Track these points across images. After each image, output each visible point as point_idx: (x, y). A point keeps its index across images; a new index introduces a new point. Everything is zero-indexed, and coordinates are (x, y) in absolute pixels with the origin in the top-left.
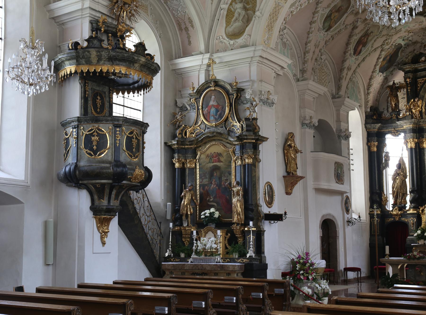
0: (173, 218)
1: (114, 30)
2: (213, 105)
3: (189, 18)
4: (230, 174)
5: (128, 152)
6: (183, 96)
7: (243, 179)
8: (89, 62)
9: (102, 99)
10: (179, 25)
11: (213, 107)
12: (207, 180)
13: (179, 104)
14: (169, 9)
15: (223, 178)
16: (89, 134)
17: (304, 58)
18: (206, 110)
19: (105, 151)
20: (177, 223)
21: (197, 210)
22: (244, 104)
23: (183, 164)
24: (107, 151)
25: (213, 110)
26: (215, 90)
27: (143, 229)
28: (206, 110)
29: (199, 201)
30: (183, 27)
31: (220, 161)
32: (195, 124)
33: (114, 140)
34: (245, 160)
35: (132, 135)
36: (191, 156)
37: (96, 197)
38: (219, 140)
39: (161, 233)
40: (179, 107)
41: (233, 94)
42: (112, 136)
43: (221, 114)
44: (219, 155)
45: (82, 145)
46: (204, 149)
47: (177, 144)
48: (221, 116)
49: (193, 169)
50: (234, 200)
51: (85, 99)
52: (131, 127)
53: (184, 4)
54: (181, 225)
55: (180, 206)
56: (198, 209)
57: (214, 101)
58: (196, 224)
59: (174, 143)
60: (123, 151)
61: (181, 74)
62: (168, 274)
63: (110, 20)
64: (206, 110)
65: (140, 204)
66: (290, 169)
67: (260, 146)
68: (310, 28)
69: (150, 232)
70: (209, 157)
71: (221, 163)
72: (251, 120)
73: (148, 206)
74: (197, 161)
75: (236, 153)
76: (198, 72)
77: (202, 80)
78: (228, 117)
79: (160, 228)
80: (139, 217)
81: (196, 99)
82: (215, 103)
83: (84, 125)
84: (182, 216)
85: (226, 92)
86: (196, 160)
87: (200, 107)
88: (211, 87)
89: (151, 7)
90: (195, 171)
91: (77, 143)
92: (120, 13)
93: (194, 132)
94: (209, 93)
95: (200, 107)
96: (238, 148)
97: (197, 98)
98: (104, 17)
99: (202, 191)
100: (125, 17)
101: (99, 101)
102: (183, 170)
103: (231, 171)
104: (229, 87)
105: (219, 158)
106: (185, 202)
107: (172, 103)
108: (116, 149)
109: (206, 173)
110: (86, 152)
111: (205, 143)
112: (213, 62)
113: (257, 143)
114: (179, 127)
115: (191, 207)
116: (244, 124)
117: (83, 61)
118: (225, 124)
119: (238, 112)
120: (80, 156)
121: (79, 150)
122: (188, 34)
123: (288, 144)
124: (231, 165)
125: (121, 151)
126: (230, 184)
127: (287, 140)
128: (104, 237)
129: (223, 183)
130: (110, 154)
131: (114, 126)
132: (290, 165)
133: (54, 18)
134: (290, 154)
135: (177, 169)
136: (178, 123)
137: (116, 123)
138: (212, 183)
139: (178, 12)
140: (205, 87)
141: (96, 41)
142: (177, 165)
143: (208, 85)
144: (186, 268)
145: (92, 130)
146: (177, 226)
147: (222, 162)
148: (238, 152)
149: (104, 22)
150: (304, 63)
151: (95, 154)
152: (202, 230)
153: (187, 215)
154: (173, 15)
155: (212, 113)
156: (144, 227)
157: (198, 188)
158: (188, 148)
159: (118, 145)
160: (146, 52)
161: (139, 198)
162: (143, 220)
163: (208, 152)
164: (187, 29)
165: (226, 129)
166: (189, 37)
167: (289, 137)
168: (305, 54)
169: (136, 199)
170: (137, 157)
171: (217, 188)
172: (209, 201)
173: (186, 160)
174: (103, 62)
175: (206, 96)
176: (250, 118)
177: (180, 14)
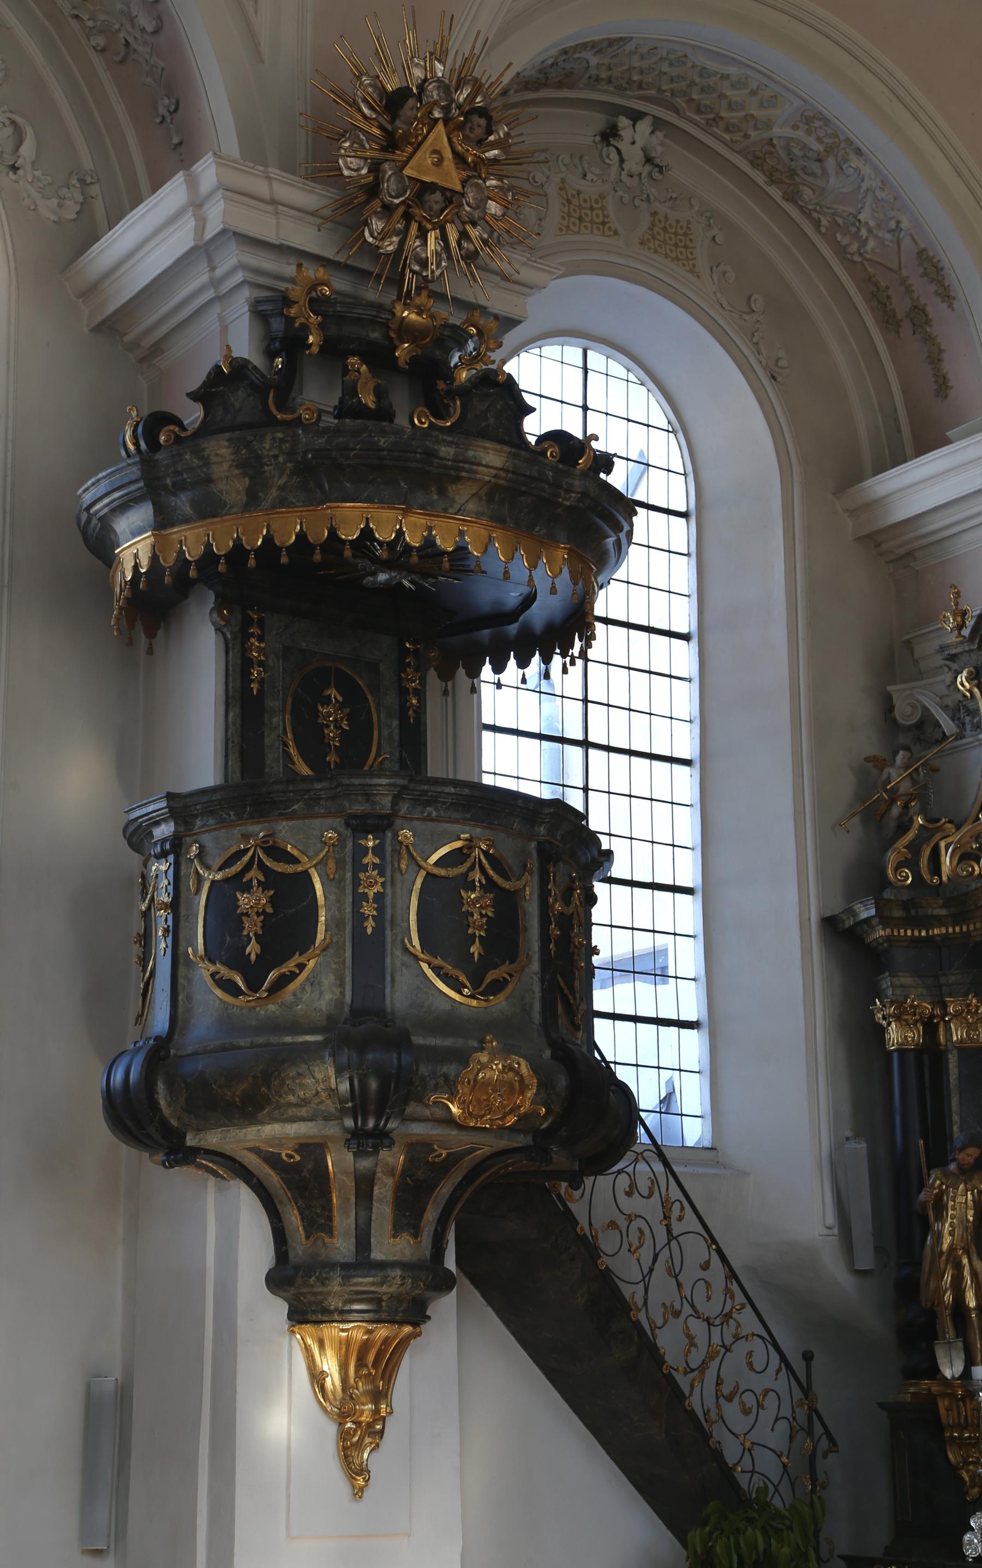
1: (375, 335)
3: (922, 254)
5: (438, 961)
8: (209, 509)
9: (354, 701)
10: (878, 299)
13: (904, 713)
14: (817, 224)
16: (226, 880)
19: (302, 967)
23: (930, 1027)
24: (311, 964)
27: (679, 1396)
30: (900, 306)
33: (349, 899)
35: (462, 869)
37: (293, 1219)
40: (909, 728)
42: (342, 879)
45: (193, 944)
51: (245, 709)
52: (457, 827)
53: (884, 183)
55: (919, 1264)
59: (864, 915)
60: (406, 959)
61: (909, 554)
63: (342, 283)
65: (646, 1255)
73: (706, 1266)
79: (807, 1391)
80: (637, 1325)
83: (206, 839)
84: (932, 1315)
89: (715, 231)
91: (175, 932)
92: (402, 243)
98: (312, 272)
100: (432, 260)
101: (331, 714)
106: (948, 1233)
108: (369, 952)
110: (213, 975)
114: (903, 827)
117: (183, 503)
120: (189, 998)
121: (182, 971)
122: (929, 339)
125: (394, 957)
128: (359, 1446)
130: (328, 980)
131: (348, 825)
133: (111, 327)
135: (895, 1055)
137: (359, 808)
139: (864, 233)
141: (241, 394)
142: (894, 1035)
145: (240, 854)
149: (317, 304)
151: (254, 986)
154: (841, 252)
156: (683, 1382)
158: (945, 937)
159: (370, 926)
160: (533, 427)
161: (630, 1218)
162: (669, 1341)
164: (919, 317)
166: (935, 357)
169: (613, 1225)
170: (497, 987)
173: (944, 1006)
174: (274, 493)
177: (871, 244)
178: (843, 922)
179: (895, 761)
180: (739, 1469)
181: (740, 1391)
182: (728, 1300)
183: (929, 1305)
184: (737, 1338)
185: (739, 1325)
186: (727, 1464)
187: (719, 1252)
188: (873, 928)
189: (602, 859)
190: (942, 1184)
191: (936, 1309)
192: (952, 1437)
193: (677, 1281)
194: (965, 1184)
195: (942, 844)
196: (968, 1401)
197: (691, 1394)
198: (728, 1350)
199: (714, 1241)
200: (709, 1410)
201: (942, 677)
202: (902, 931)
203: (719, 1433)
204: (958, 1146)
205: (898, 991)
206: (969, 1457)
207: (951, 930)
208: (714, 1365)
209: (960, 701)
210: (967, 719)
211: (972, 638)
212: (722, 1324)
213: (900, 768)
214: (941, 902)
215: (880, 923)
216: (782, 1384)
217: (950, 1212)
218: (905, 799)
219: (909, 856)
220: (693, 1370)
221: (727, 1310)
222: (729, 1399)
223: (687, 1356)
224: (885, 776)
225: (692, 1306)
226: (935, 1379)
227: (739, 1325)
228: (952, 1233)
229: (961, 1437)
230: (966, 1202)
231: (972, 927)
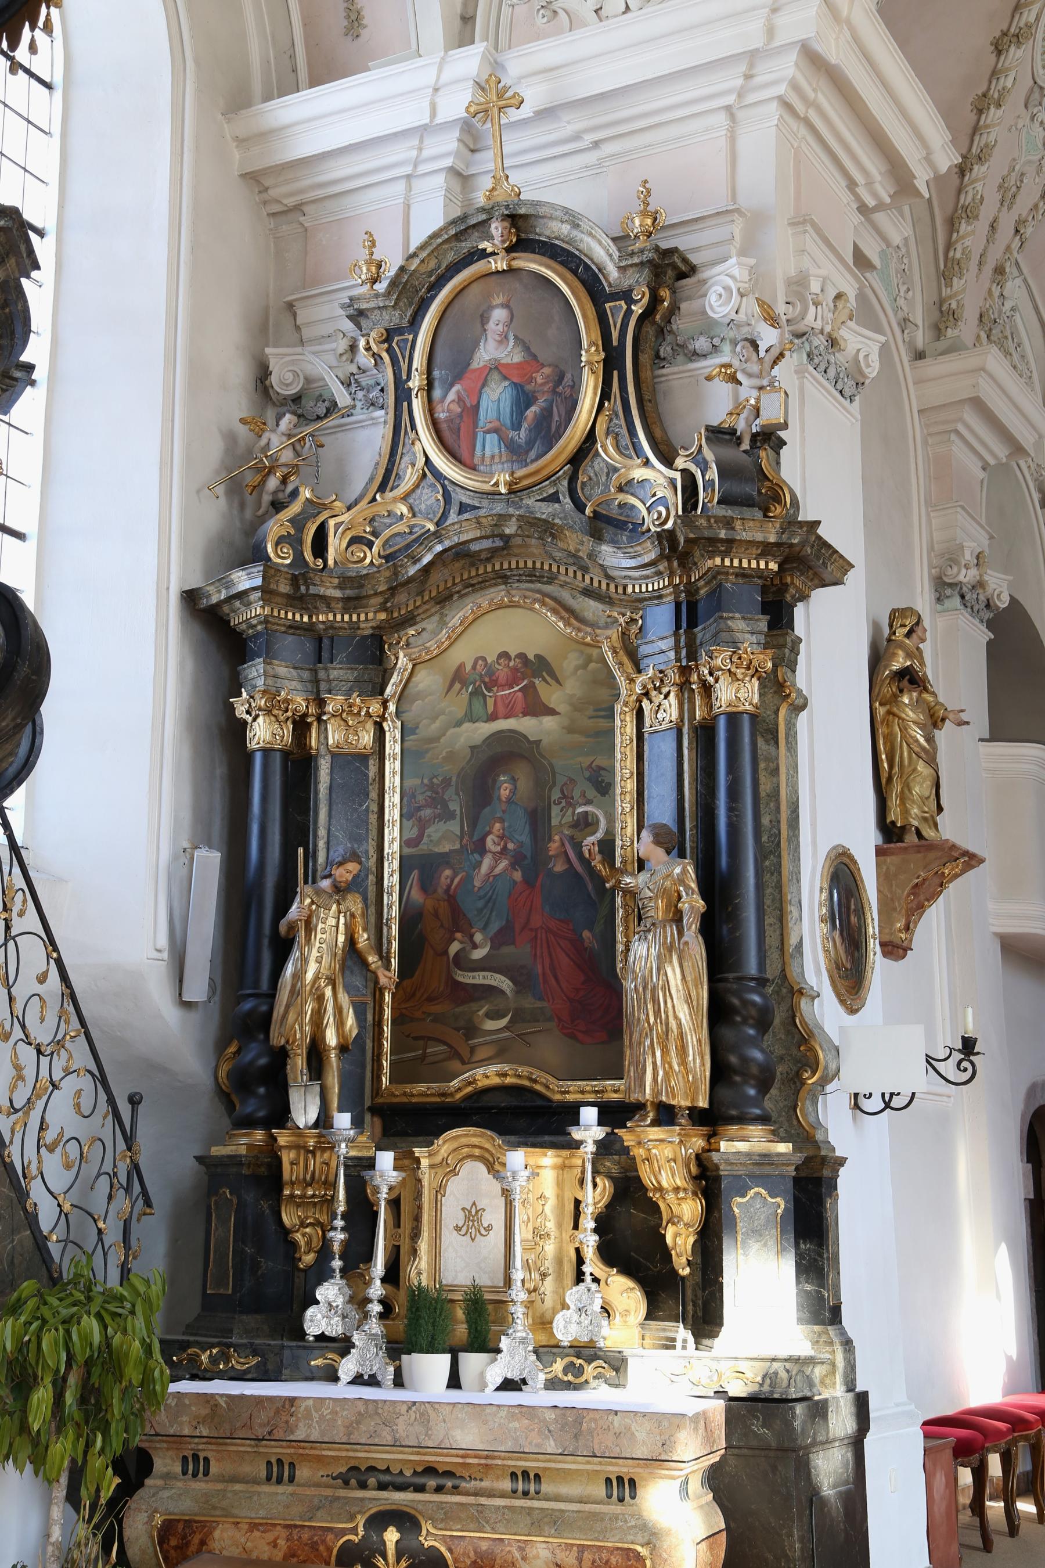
0: (222, 1073)
2: (497, 368)
4: (603, 786)
6: (306, 333)
7: (695, 816)
11: (496, 376)
12: (454, 827)
13: (284, 380)
15: (555, 810)
17: (949, 246)
18: (452, 396)
20: (250, 1107)
21: (378, 1024)
22: (696, 355)
25: (496, 398)
26: (511, 271)
28: (449, 401)
29: (394, 962)
31: (536, 708)
32: (382, 488)
34: (707, 689)
36: (351, 675)
38: (533, 576)
39: (135, 1168)
41: (627, 296)
43: (546, 415)
44: (535, 668)
46: (428, 635)
47: (267, 592)
48: (547, 432)
49: (363, 758)
50: (641, 954)
54: (279, 1115)
56: (388, 1013)
57: (504, 339)
58: (374, 1110)
61: (298, 208)
62: (167, 1476)
64: (452, 396)
66: (906, 812)
67: (799, 611)
68: (995, 74)
69: (52, 1163)
70: (464, 684)
71: (548, 722)
72: (746, 445)
73: (42, 979)
74: (392, 707)
75: (644, 650)
76: (400, 187)
77: (430, 216)
78: (591, 437)
79: (130, 1141)
81: (388, 336)
82: (511, 355)
84: (281, 1056)
85: (583, 282)
86: (385, 704)
87: (416, 382)
88: (483, 254)
90: (373, 771)
93: (375, 534)
94: (475, 288)
95: (416, 382)
96: (660, 619)
97: (399, 330)
99: (416, 895)
102: (297, 764)
103: (612, 771)
104: (601, 252)
105: (530, 691)
107: (239, 374)
109: (447, 782)
111: (444, 599)
112: (500, 96)
113: (784, 588)
115: (344, 999)
116: (705, 468)
118: (573, 479)
119: (653, 400)
123: (896, 666)
124: (612, 731)
126: (607, 847)
127: (876, 660)
129: (554, 847)
132: (907, 786)
134: (904, 729)
135: (258, 758)
136: (273, 483)
138: (481, 848)
140: (450, 257)
142: (262, 732)
143: (466, 246)
144: (300, 1434)
146: (247, 1123)
147: (552, 712)
148: (663, 645)
150: (948, 269)
152: (418, 1152)
153: (316, 1054)
155: (492, 415)
157: (392, 879)
158: (330, 626)
163: (463, 654)
165: (580, 507)
167: (901, 632)
168: (952, 224)
171: (518, 876)
172: (461, 961)
173: (321, 703)
175: (456, 305)
176: (741, 426)
178: (209, 596)
179: (278, 425)
180: (54, 1238)
181: (64, 1139)
182: (62, 1023)
183: (283, 1042)
184: (68, 1072)
185: (70, 1057)
186: (41, 1232)
187: (60, 963)
188: (248, 604)
189: (18, 374)
190: (313, 902)
191: (288, 1047)
192: (292, 1196)
193: (9, 993)
194: (339, 904)
195: (332, 523)
196: (318, 1154)
197: (11, 1142)
198: (55, 1086)
199: (56, 949)
200: (30, 1162)
201: (334, 345)
202: (283, 612)
203: (37, 1193)
205: (270, 682)
206: (307, 1218)
207: (339, 618)
208: (40, 1104)
209: (352, 374)
210: (360, 394)
211: (388, 293)
212: (52, 1053)
213: (283, 434)
214: (336, 581)
215: (262, 599)
216: (107, 1130)
217: (319, 936)
218: (286, 470)
219: (292, 532)
220: (16, 1111)
221: (59, 1037)
222: (51, 1149)
223: (12, 1092)
224: (263, 442)
225: (23, 1027)
227: (70, 1057)
229: (303, 1196)
230: (337, 926)
231: (363, 617)
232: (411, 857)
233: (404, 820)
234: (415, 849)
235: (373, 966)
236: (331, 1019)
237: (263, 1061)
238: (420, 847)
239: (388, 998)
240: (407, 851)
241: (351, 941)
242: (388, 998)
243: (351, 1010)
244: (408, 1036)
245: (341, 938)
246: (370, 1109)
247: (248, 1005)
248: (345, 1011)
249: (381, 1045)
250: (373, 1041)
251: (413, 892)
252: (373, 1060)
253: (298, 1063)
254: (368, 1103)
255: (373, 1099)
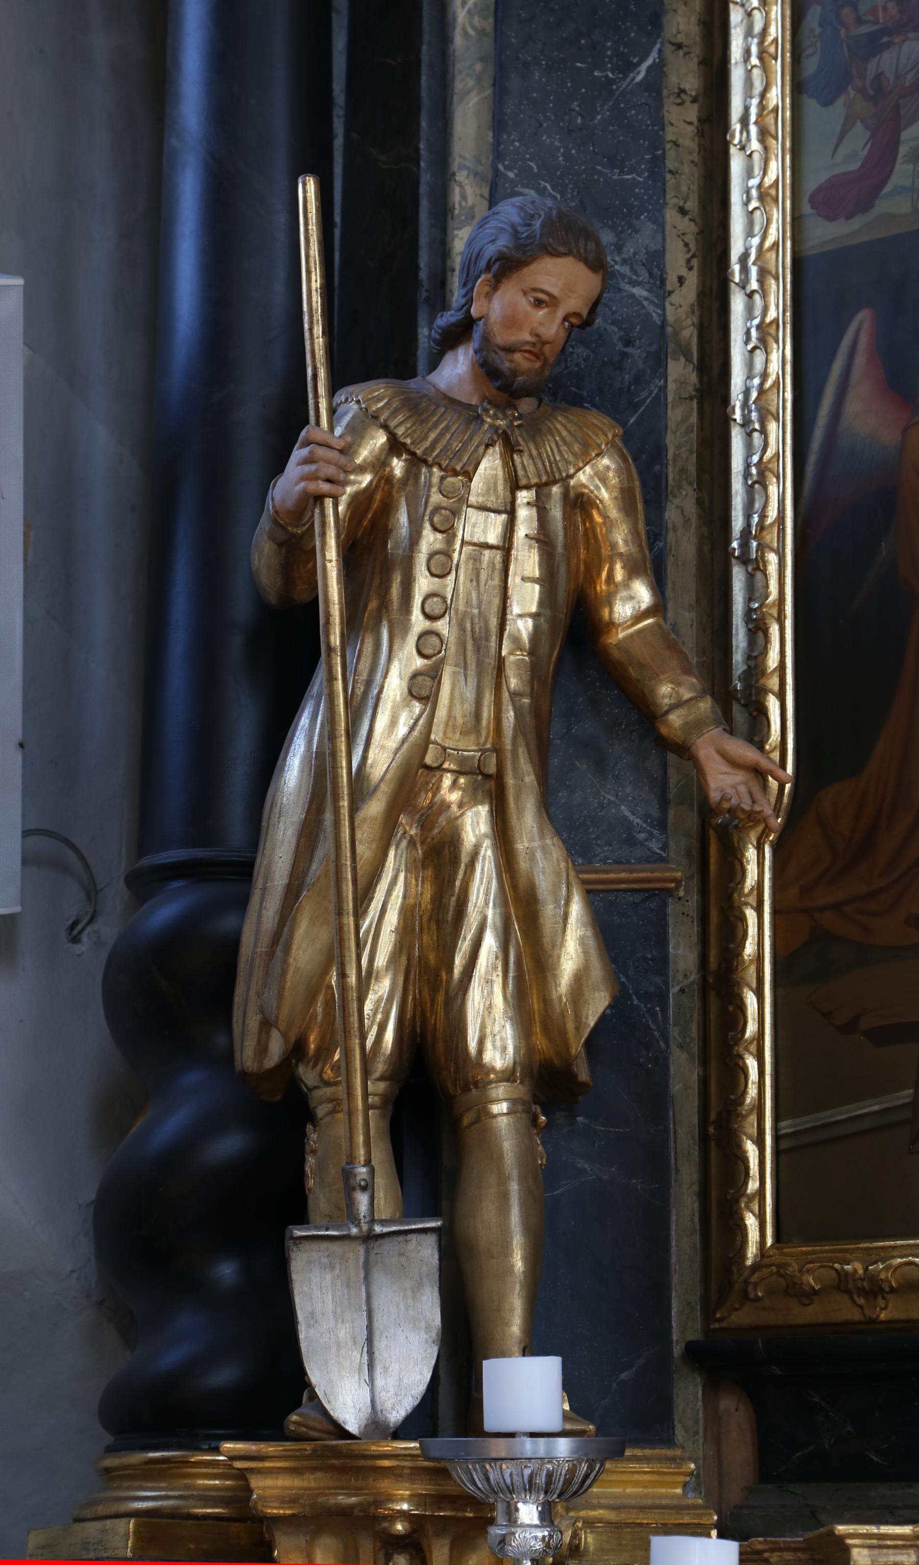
21: (721, 983)
29: (779, 713)
55: (238, 872)
56: (757, 936)
58: (721, 1361)
84: (283, 1111)
99: (866, 417)
106: (393, 708)
115: (542, 854)
153: (428, 1091)
157: (760, 364)
183: (276, 1047)
190: (395, 446)
191: (307, 1075)
194: (510, 449)
204: (490, 251)
217: (423, 583)
226: (278, 1433)
228: (423, 689)
230: (506, 547)
232: (841, 258)
233: (811, 105)
234: (858, 222)
235: (676, 719)
236: (490, 942)
237: (229, 1146)
238: (882, 206)
239: (756, 867)
240: (824, 233)
241: (575, 621)
242: (756, 867)
243: (576, 908)
244: (851, 1027)
245: (526, 598)
246: (696, 1353)
247: (166, 911)
248: (549, 911)
249: (734, 1073)
250: (704, 1061)
251: (853, 406)
252: (704, 1139)
253: (355, 1142)
254: (684, 1325)
255: (708, 1310)
